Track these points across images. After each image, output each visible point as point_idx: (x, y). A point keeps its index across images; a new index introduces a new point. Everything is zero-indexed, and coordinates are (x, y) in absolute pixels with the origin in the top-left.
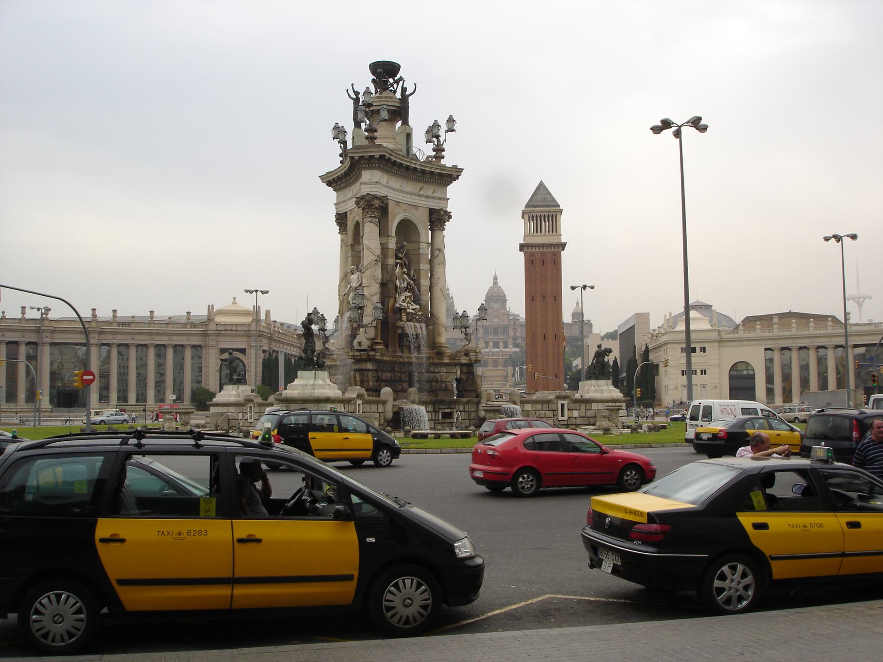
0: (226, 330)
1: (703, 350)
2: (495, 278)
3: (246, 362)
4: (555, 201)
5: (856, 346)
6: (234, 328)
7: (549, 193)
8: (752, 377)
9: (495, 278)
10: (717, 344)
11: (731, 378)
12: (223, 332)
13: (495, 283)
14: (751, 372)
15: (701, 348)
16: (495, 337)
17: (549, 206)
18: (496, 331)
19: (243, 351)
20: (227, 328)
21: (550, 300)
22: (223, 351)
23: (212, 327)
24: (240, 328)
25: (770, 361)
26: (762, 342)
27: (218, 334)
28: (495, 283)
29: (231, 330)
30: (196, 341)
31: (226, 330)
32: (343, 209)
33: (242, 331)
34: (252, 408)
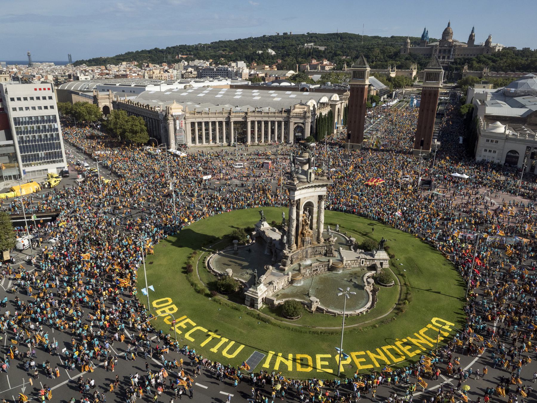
2: (449, 24)
8: (518, 158)
9: (449, 24)
11: (507, 156)
14: (517, 155)
22: (295, 123)
23: (292, 114)
27: (293, 117)
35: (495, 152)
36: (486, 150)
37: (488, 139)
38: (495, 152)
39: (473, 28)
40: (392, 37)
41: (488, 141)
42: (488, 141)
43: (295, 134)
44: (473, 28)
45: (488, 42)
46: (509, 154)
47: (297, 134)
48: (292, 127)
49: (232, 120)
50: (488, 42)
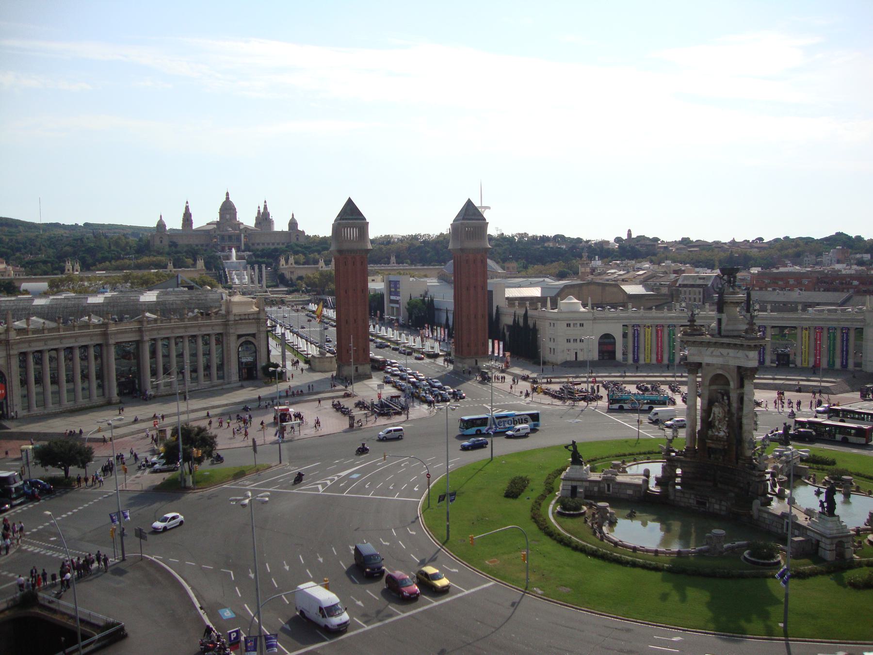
0: (241, 319)
1: (581, 325)
2: (227, 194)
3: (256, 344)
6: (247, 317)
8: (614, 344)
9: (227, 194)
10: (591, 322)
11: (600, 344)
13: (228, 198)
14: (612, 340)
15: (580, 324)
16: (229, 243)
17: (477, 220)
18: (230, 237)
19: (254, 335)
22: (239, 336)
23: (232, 318)
24: (251, 317)
25: (625, 335)
26: (621, 321)
28: (228, 198)
29: (245, 319)
30: (218, 330)
31: (241, 319)
32: (696, 359)
33: (253, 319)
34: (611, 485)
36: (568, 341)
37: (568, 322)
39: (265, 202)
40: (86, 224)
41: (568, 325)
42: (568, 325)
44: (265, 202)
45: (293, 224)
46: (602, 341)
47: (244, 360)
48: (233, 344)
49: (112, 341)
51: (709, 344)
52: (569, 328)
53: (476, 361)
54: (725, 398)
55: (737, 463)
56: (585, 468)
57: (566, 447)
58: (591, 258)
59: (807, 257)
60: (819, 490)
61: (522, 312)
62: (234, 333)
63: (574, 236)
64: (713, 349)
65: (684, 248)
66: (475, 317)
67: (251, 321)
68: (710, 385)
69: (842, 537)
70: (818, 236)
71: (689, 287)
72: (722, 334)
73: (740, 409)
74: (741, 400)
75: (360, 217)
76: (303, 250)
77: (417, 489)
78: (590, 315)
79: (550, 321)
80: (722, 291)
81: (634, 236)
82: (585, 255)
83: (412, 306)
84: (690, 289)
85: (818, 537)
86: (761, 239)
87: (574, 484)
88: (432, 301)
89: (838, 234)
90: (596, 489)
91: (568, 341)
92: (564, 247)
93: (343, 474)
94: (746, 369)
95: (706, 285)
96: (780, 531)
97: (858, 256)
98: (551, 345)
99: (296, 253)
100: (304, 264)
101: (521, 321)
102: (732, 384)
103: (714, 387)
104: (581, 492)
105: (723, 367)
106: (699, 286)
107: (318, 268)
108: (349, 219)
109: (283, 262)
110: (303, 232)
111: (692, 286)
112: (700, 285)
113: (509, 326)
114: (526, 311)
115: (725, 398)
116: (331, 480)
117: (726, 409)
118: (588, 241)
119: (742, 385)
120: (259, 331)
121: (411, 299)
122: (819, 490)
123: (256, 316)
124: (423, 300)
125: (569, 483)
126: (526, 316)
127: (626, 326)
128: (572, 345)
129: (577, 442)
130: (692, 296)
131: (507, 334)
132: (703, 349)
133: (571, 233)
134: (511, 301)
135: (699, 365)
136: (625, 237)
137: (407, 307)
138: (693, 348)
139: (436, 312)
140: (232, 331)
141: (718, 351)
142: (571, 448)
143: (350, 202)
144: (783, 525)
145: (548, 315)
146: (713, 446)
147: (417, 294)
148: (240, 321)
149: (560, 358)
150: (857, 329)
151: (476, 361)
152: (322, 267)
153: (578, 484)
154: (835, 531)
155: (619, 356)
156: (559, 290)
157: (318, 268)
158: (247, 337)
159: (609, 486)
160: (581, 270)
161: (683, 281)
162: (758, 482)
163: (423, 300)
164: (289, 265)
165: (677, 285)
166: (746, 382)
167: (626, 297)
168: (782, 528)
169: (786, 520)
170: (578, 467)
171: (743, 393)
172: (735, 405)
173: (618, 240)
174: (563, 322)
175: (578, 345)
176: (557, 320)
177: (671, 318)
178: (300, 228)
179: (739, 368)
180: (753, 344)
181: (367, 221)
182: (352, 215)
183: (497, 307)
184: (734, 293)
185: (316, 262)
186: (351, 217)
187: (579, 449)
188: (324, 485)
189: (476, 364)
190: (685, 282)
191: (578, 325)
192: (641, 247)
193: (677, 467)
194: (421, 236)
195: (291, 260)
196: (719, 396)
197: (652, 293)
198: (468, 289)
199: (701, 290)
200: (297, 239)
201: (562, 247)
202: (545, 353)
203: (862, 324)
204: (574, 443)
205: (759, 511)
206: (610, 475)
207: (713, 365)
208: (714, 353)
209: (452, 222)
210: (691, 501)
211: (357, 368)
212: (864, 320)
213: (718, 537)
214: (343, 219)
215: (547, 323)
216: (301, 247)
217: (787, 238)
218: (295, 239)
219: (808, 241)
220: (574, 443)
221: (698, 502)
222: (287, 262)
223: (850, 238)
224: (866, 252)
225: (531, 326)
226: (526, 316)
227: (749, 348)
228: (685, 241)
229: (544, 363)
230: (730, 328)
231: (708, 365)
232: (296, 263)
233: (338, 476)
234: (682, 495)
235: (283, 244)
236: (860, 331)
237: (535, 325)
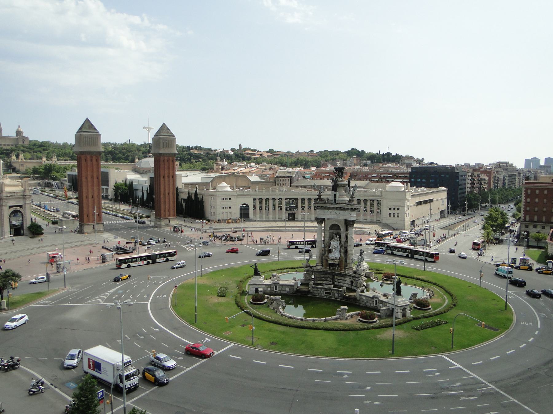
1: (230, 199)
4: (172, 134)
5: (286, 199)
6: (16, 194)
7: (168, 129)
8: (248, 209)
10: (236, 197)
12: (11, 197)
17: (170, 136)
19: (21, 206)
20: (12, 194)
21: (171, 177)
22: (10, 207)
24: (19, 194)
27: (8, 198)
29: (14, 196)
35: (230, 208)
36: (223, 208)
38: (230, 208)
41: (223, 199)
42: (223, 199)
43: (10, 222)
50: (18, 133)
51: (329, 208)
52: (223, 200)
53: (169, 220)
54: (338, 236)
55: (345, 271)
56: (262, 277)
57: (251, 266)
58: (221, 159)
59: (339, 162)
60: (382, 284)
61: (193, 191)
62: (6, 205)
63: (206, 147)
64: (331, 211)
65: (272, 155)
66: (169, 194)
67: (19, 197)
68: (330, 229)
69: (405, 306)
70: (343, 150)
71: (283, 177)
72: (337, 203)
73: (346, 242)
74: (347, 237)
75: (95, 131)
76: (29, 150)
77: (146, 297)
78: (235, 194)
79: (212, 197)
80: (337, 180)
81: (242, 148)
82: (219, 158)
83: (117, 188)
84: (283, 179)
85: (393, 306)
86: (312, 151)
87: (257, 287)
88: (132, 183)
89: (353, 149)
90: (269, 289)
91: (223, 208)
92: (202, 153)
93: (112, 291)
94: (350, 221)
95: (292, 176)
96: (372, 305)
97: (365, 161)
98: (213, 210)
99: (23, 151)
100: (30, 159)
101: (193, 197)
102: (342, 229)
103: (331, 231)
104: (261, 291)
105: (337, 220)
106: (288, 177)
107: (41, 162)
108: (88, 132)
109: (14, 157)
110: (27, 138)
111: (284, 177)
112: (289, 176)
113: (185, 200)
114: (196, 190)
115: (338, 236)
116: (106, 295)
117: (339, 242)
118: (215, 150)
119: (347, 230)
120: (25, 204)
121: (116, 183)
122: (382, 284)
123: (22, 194)
124: (126, 184)
125: (254, 286)
126: (196, 193)
127: (255, 199)
128: (225, 210)
129: (257, 263)
130: (284, 183)
131: (184, 204)
132: (326, 211)
133: (205, 145)
134: (186, 184)
135: (324, 220)
136: (237, 148)
137: (114, 188)
138: (320, 210)
139: (135, 192)
140: (4, 204)
141: (334, 212)
142: (254, 267)
143: (87, 121)
144: (373, 302)
145: (210, 193)
146: (332, 262)
147: (120, 181)
148: (11, 197)
149: (219, 217)
150: (378, 200)
151: (169, 220)
152: (44, 162)
153: (259, 286)
154: (402, 303)
155: (251, 215)
156: (212, 179)
157: (41, 162)
158: (16, 207)
159: (276, 287)
160: (215, 166)
161: (279, 174)
162: (358, 280)
163: (126, 184)
164: (20, 160)
165: (276, 176)
166: (349, 228)
167: (250, 183)
168: (373, 304)
169: (375, 299)
170: (258, 277)
171: (348, 234)
172: (343, 240)
173: (233, 150)
174: (220, 197)
175: (228, 210)
176: (216, 196)
177: (280, 195)
178: (25, 135)
179: (346, 220)
180: (354, 208)
181: (100, 133)
182: (89, 128)
183: (177, 187)
184: (342, 181)
185: (41, 158)
186: (89, 131)
187: (258, 268)
188: (102, 299)
189: (169, 222)
190: (280, 175)
191: (228, 199)
192: (247, 154)
193: (312, 275)
194: (110, 144)
195: (21, 156)
196: (335, 236)
197: (263, 181)
198: (164, 177)
199: (290, 179)
200: (23, 142)
201: (201, 153)
202: (208, 215)
203: (380, 198)
204: (255, 264)
205: (360, 295)
206: (276, 281)
207: (331, 219)
208: (332, 213)
209: (153, 137)
210: (322, 293)
211: (94, 226)
212: (381, 196)
213: (345, 310)
214: (84, 132)
215: (210, 198)
216: (26, 148)
217: (326, 151)
218: (22, 142)
219: (338, 153)
220: (255, 264)
221: (326, 293)
222: (17, 157)
223: (359, 152)
224: (368, 160)
225: (200, 200)
226: (196, 193)
227: (352, 210)
228: (271, 151)
229: (209, 221)
230: (341, 199)
231: (328, 219)
232: (25, 158)
233: (110, 293)
234: (317, 290)
235: (12, 145)
236: (379, 202)
237: (202, 199)
